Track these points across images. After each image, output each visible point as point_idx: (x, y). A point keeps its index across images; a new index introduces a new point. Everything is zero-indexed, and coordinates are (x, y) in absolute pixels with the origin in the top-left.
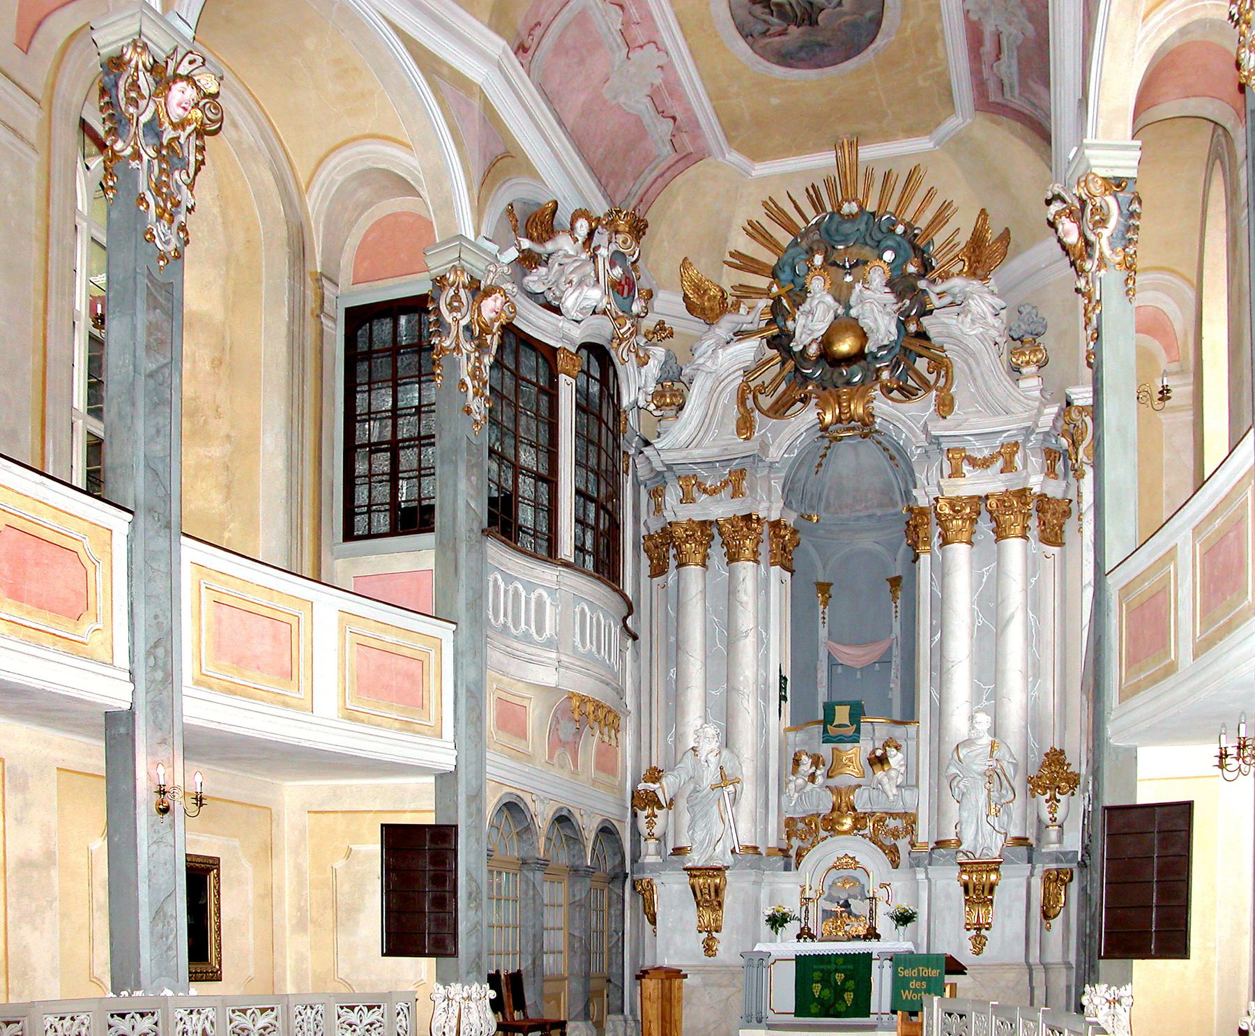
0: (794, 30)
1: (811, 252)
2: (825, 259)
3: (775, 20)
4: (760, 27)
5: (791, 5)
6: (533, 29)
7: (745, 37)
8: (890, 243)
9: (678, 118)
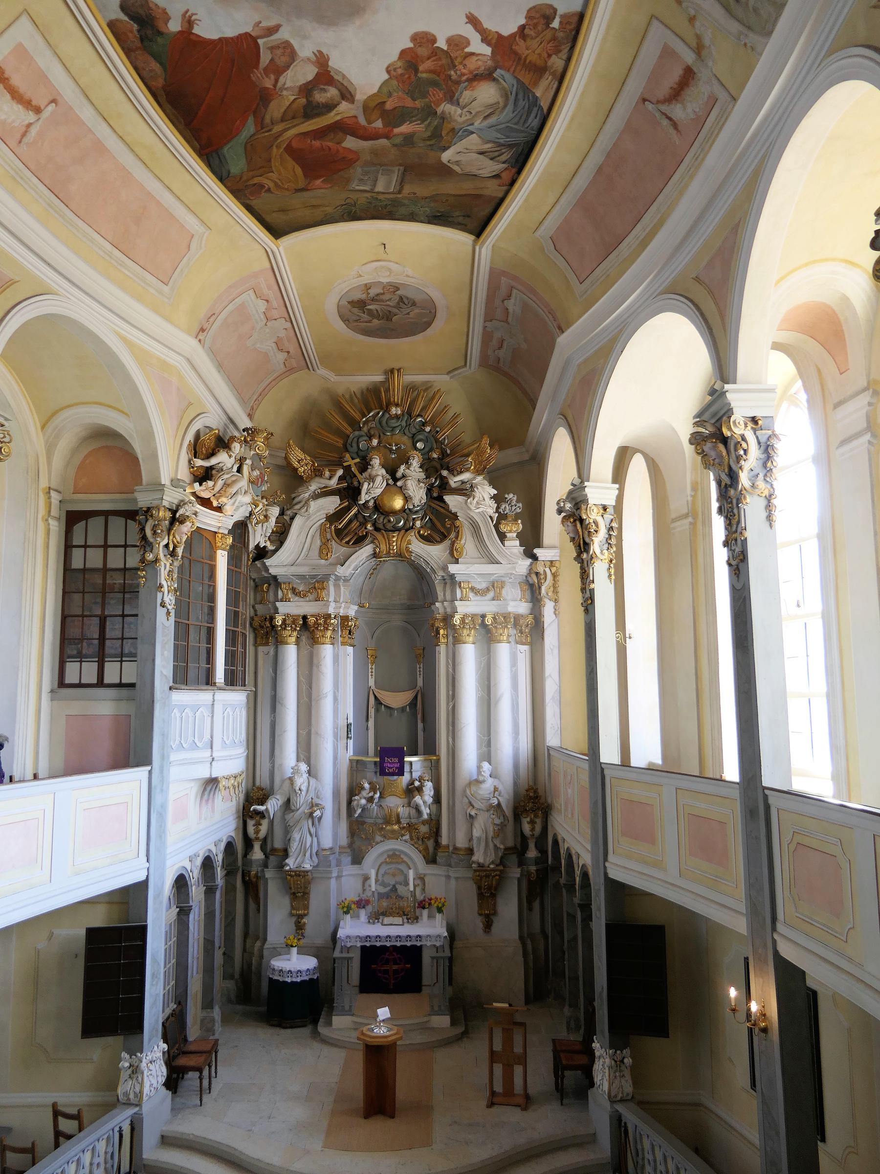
0: (376, 322)
1: (370, 437)
2: (379, 443)
3: (365, 316)
4: (355, 318)
5: (377, 310)
6: (209, 318)
7: (344, 321)
8: (421, 437)
9: (291, 352)
